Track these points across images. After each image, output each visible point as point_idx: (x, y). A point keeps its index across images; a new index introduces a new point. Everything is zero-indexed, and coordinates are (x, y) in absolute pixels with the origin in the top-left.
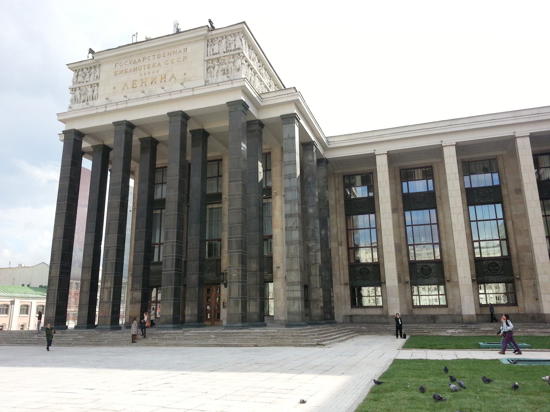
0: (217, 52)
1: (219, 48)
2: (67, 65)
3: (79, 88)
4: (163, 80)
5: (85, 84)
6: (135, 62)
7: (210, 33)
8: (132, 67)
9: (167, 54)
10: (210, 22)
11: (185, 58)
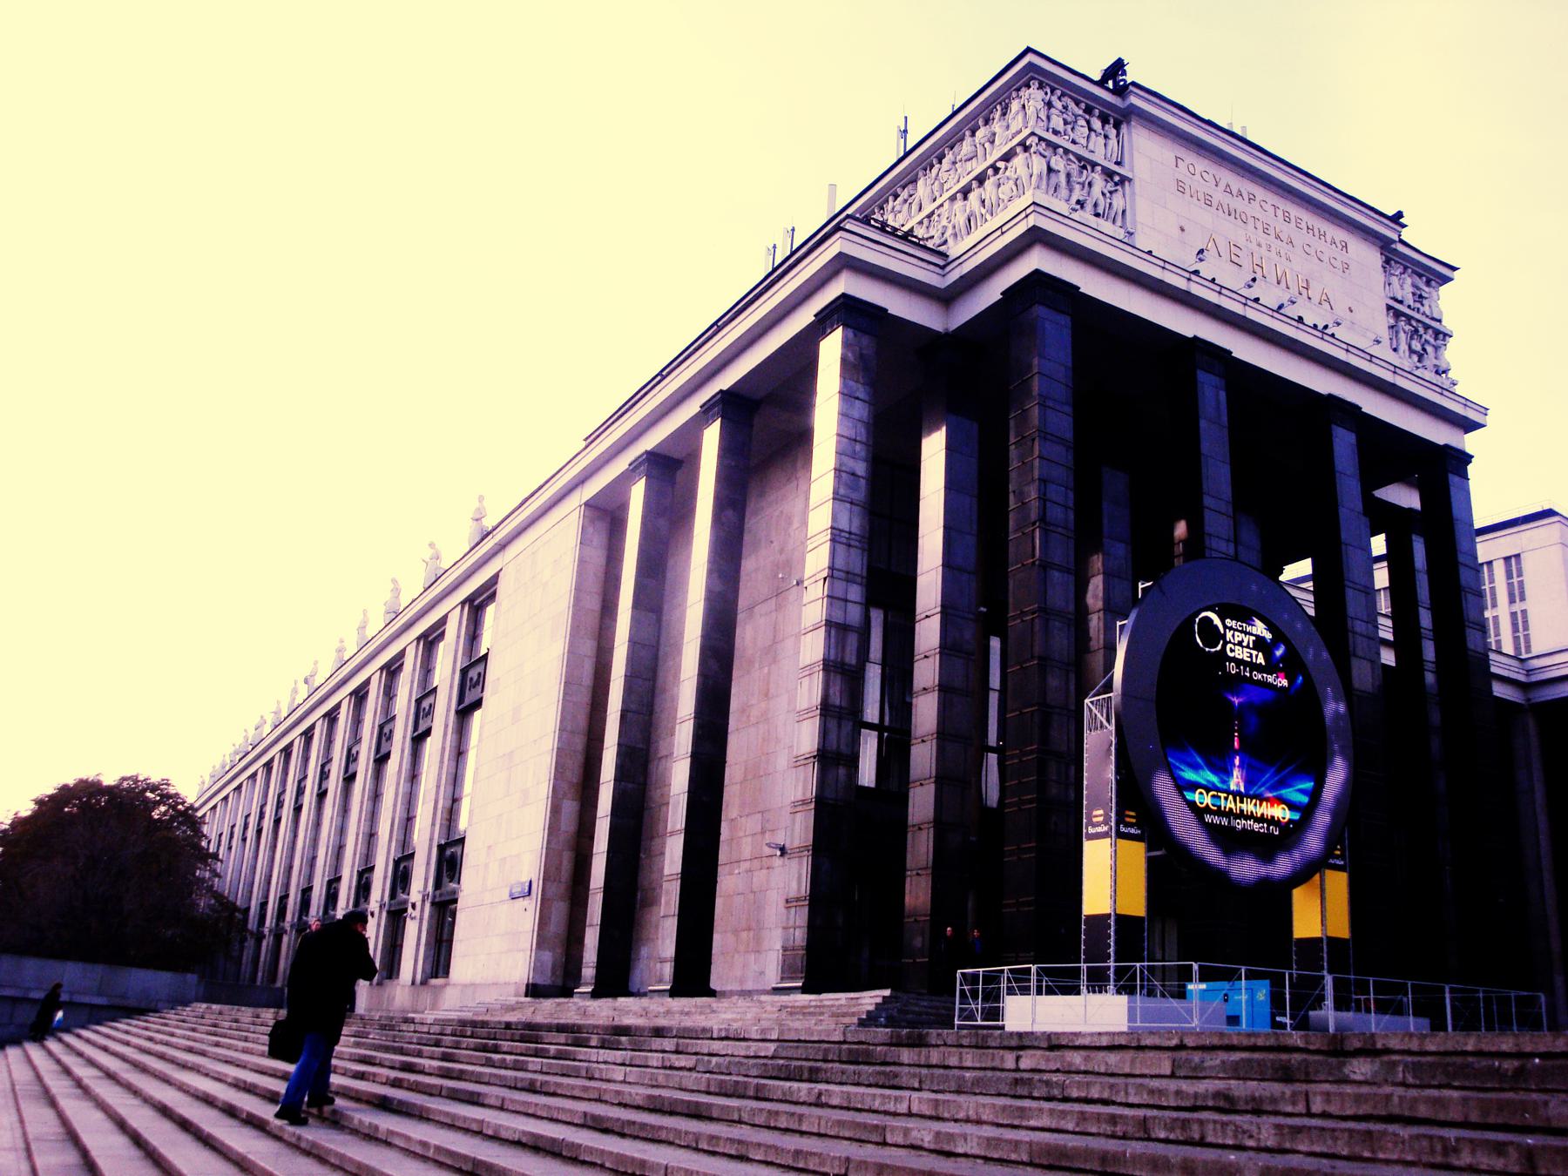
1: (1404, 288)
3: (1066, 151)
6: (1228, 190)
8: (1218, 196)
11: (1346, 267)
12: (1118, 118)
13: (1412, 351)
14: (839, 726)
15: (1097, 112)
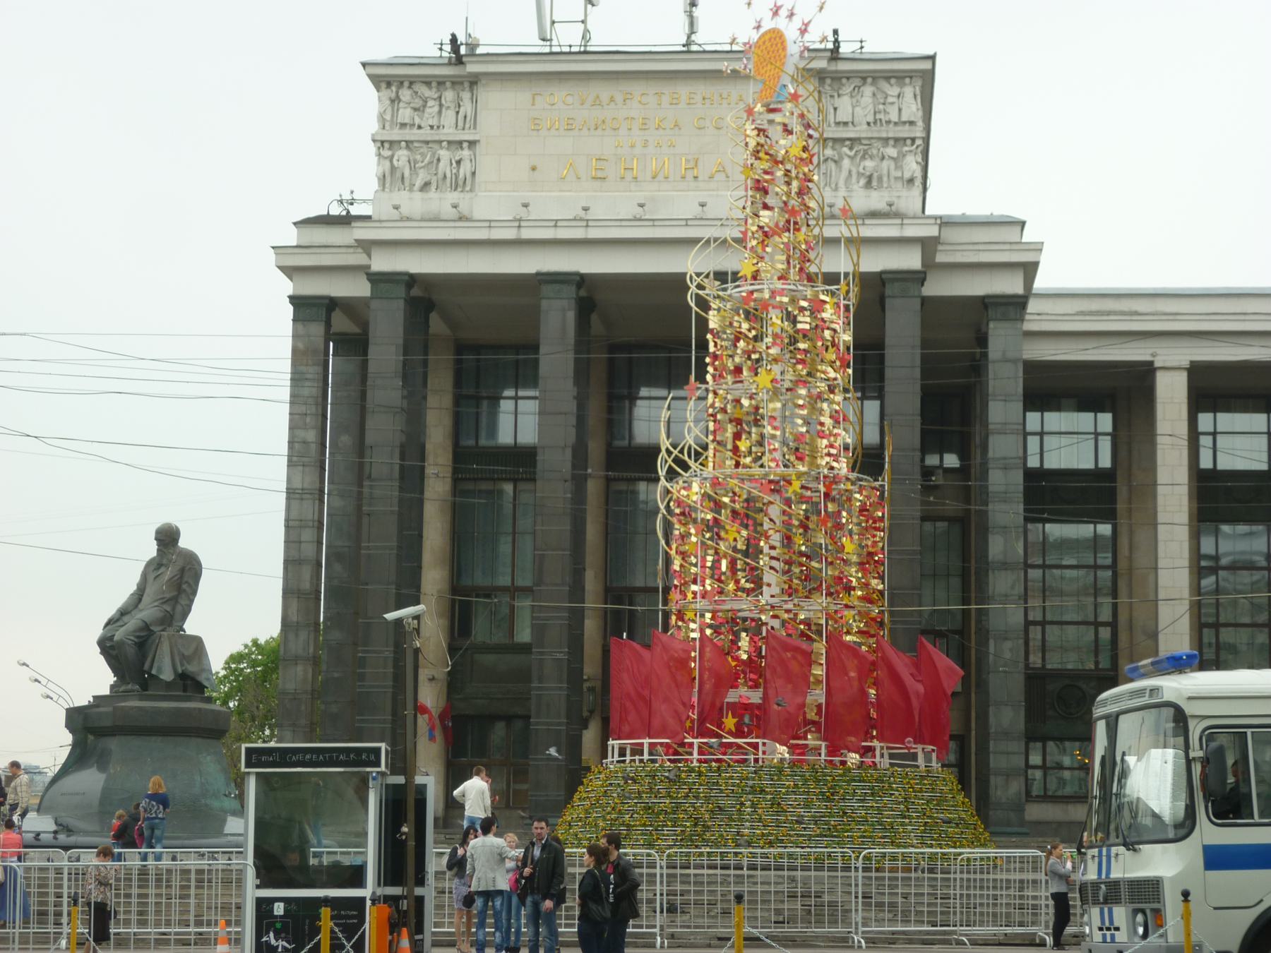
0: (847, 118)
2: (364, 65)
4: (690, 174)
5: (426, 134)
6: (597, 102)
7: (834, 67)
9: (698, 98)
10: (836, 32)
12: (474, 81)
13: (860, 175)
14: (297, 635)
15: (448, 84)
